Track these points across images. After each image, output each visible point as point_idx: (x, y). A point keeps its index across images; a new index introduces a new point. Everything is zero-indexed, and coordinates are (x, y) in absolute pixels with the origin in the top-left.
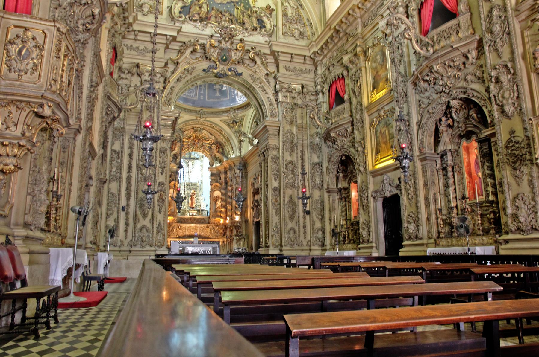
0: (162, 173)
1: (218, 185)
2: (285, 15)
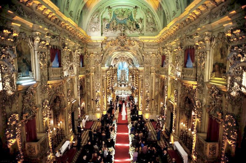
1: (131, 74)
2: (147, 21)
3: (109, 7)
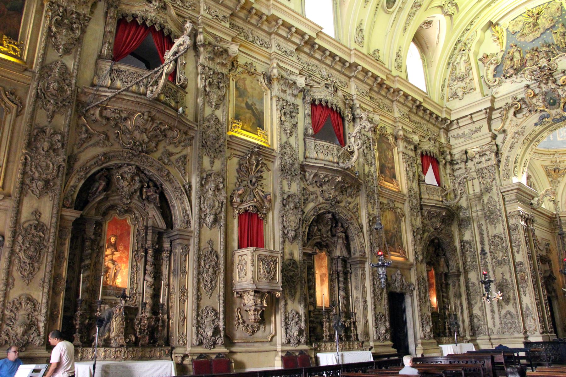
0: (518, 252)
3: (491, 24)
